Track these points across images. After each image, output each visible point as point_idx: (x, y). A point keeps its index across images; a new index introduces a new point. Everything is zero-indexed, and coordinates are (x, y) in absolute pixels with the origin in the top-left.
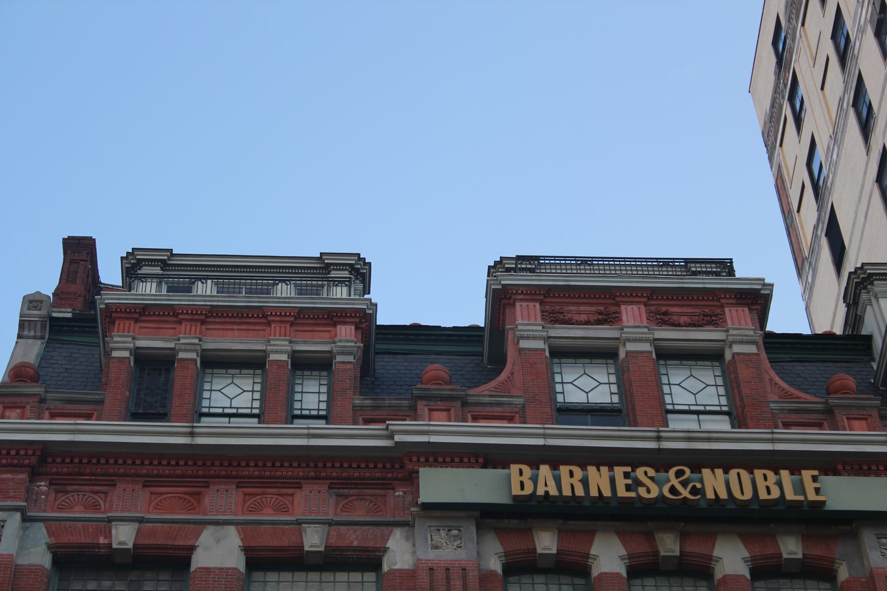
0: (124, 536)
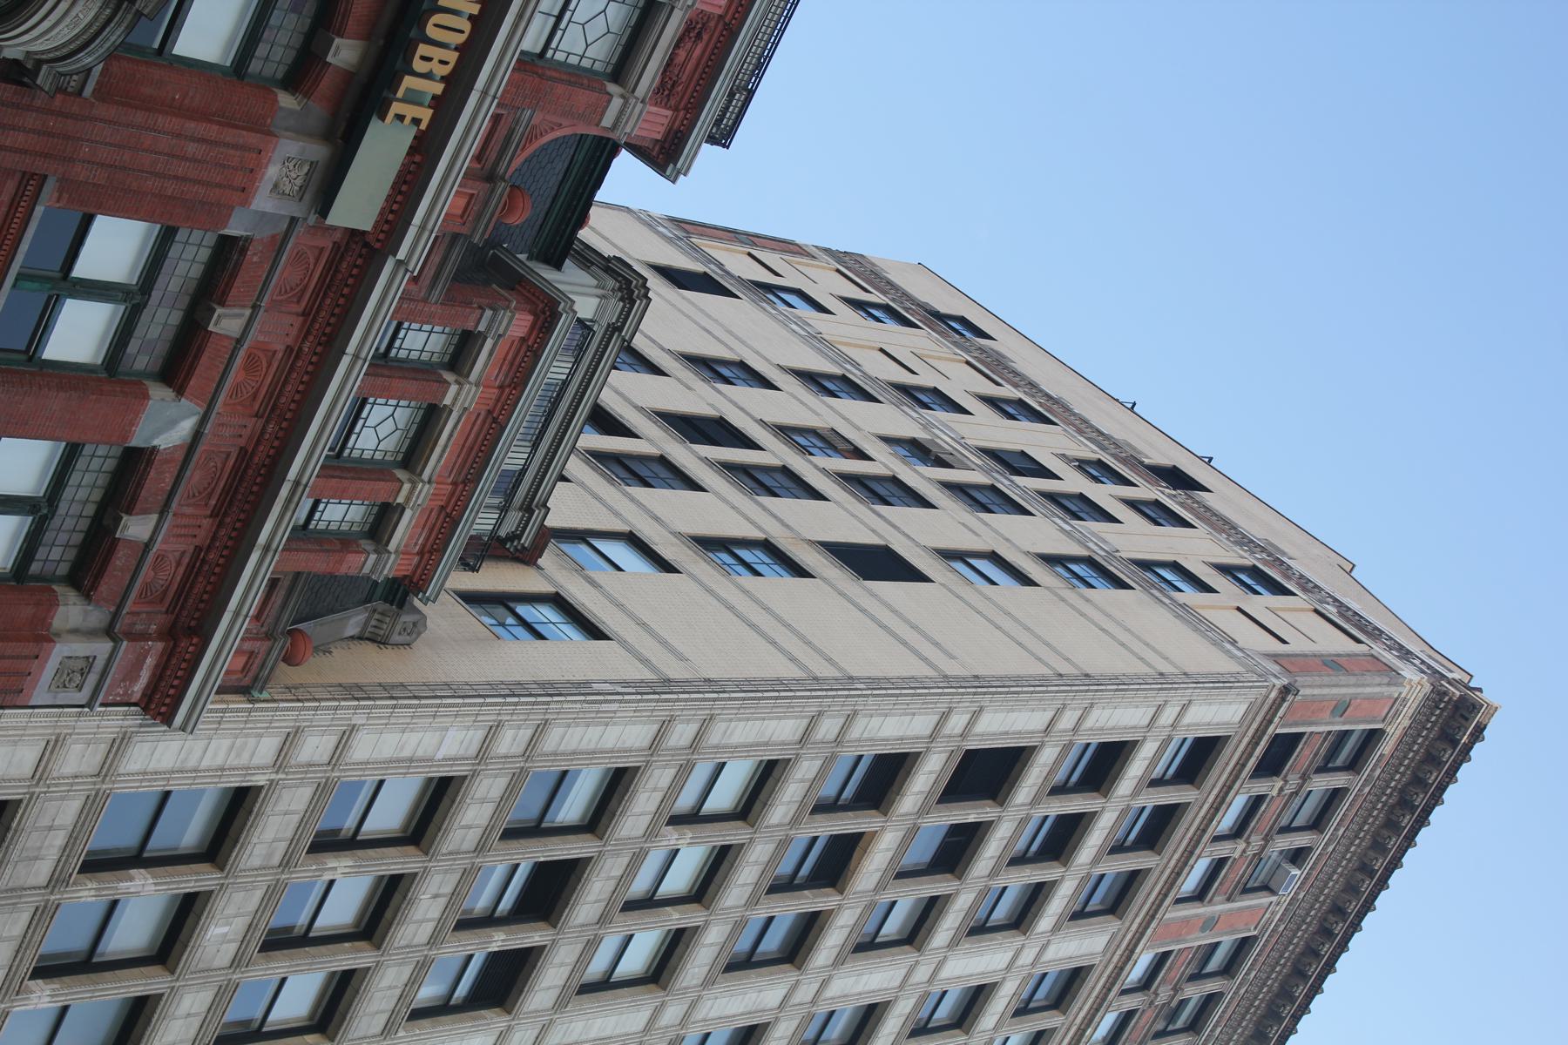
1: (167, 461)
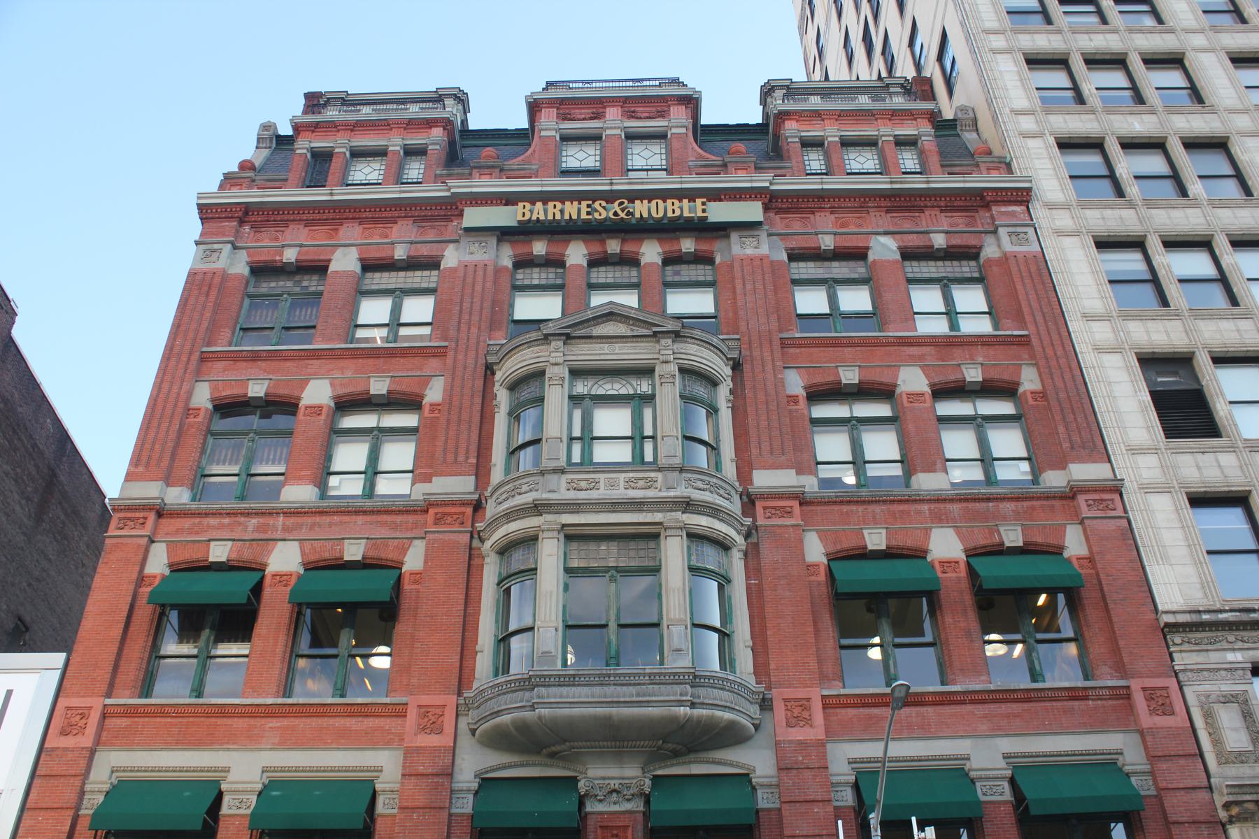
0: (290, 255)
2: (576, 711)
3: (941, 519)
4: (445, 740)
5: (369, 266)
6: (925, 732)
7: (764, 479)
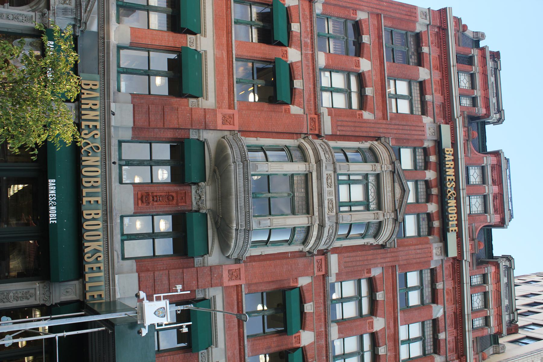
0: (425, 50)
1: (441, 319)
2: (233, 181)
3: (318, 336)
4: (220, 125)
5: (422, 84)
6: (227, 329)
7: (334, 259)
